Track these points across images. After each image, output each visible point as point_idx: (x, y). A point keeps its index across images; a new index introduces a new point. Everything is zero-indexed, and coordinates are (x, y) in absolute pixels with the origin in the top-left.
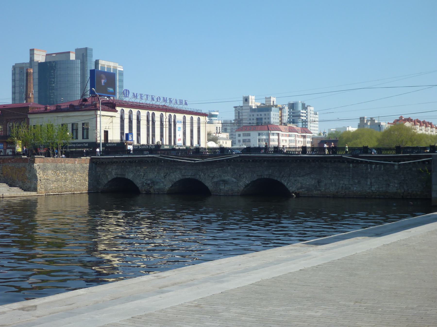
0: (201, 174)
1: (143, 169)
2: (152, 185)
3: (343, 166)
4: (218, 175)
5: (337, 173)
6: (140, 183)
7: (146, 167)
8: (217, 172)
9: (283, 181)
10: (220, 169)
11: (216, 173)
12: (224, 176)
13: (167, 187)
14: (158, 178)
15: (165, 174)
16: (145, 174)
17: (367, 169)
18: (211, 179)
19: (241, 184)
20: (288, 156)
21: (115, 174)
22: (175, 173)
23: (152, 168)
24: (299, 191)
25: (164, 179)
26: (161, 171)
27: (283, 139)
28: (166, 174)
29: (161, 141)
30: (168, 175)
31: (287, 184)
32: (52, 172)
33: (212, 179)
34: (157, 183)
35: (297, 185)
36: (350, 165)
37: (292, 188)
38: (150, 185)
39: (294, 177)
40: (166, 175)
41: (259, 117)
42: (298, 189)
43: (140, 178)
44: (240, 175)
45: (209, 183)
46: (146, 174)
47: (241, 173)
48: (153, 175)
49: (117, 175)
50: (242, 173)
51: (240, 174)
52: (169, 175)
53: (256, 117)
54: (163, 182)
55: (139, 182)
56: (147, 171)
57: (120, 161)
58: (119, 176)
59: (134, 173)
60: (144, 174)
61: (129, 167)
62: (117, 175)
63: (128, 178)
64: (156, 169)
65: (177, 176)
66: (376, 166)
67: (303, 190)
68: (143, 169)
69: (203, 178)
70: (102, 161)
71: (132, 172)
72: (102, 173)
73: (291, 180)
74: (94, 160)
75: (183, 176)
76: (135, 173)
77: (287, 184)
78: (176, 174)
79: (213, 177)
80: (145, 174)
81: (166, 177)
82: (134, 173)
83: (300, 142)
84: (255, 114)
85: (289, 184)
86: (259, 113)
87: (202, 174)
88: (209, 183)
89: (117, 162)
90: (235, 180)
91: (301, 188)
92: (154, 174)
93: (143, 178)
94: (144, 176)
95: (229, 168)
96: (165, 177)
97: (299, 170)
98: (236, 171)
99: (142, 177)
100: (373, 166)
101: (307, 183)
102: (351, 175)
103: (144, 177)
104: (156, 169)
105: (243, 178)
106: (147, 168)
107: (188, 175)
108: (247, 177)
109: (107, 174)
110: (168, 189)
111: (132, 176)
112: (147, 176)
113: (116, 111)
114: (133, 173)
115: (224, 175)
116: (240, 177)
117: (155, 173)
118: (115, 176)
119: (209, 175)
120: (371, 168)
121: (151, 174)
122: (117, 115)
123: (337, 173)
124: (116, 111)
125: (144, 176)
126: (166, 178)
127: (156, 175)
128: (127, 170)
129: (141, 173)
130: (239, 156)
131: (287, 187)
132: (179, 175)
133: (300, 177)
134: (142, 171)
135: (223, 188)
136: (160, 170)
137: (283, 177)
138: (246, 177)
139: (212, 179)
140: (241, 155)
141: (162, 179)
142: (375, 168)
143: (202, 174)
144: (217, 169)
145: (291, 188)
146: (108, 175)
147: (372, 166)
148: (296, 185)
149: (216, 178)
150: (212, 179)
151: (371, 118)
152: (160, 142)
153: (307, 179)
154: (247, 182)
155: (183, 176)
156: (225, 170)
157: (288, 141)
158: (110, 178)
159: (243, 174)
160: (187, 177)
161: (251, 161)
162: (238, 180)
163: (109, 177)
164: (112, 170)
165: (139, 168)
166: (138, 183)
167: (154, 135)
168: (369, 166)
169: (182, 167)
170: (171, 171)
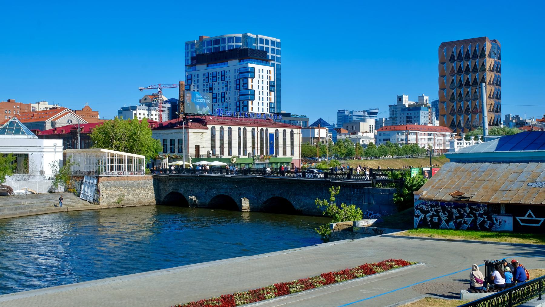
10: (245, 187)
12: (248, 194)
21: (171, 189)
27: (422, 138)
29: (252, 153)
30: (208, 191)
31: (294, 202)
32: (116, 188)
40: (207, 191)
41: (409, 115)
42: (301, 207)
44: (259, 194)
46: (193, 190)
48: (198, 191)
53: (406, 115)
62: (173, 189)
64: (200, 186)
72: (162, 188)
74: (156, 177)
77: (294, 202)
81: (207, 193)
83: (439, 141)
84: (406, 113)
86: (409, 112)
96: (206, 192)
98: (256, 190)
99: (190, 193)
104: (200, 186)
113: (207, 129)
115: (248, 192)
118: (171, 191)
120: (354, 191)
122: (208, 132)
124: (207, 129)
125: (191, 192)
134: (190, 187)
139: (239, 196)
151: (517, 116)
152: (251, 153)
157: (427, 140)
158: (168, 193)
160: (221, 193)
167: (245, 147)
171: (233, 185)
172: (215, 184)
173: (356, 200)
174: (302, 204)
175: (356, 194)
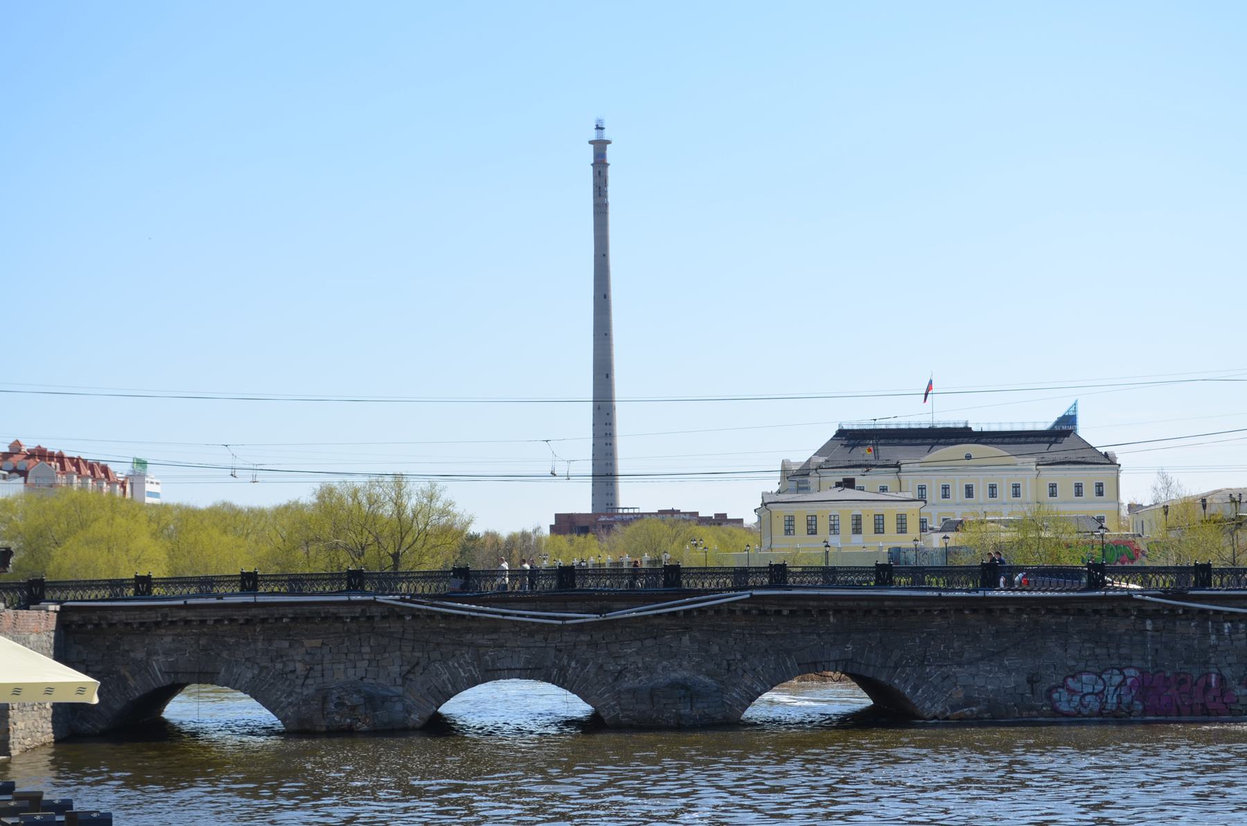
0: (569, 665)
1: (302, 651)
3: (1122, 626)
4: (640, 666)
5: (1098, 651)
6: (290, 704)
7: (317, 643)
8: (638, 654)
9: (897, 681)
10: (648, 642)
11: (631, 659)
12: (664, 668)
15: (403, 668)
16: (311, 669)
17: (1206, 635)
18: (610, 681)
19: (734, 694)
20: (935, 594)
23: (347, 643)
24: (958, 712)
25: (403, 685)
26: (387, 655)
28: (408, 668)
30: (419, 669)
31: (915, 689)
34: (383, 702)
35: (951, 695)
36: (1144, 623)
37: (932, 706)
39: (942, 666)
40: (409, 672)
43: (288, 683)
44: (729, 665)
45: (602, 694)
46: (319, 667)
48: (351, 672)
49: (172, 675)
51: (727, 660)
54: (401, 697)
55: (283, 699)
56: (323, 656)
57: (206, 620)
59: (257, 664)
60: (308, 667)
61: (232, 641)
62: (176, 673)
64: (366, 649)
65: (463, 674)
66: (1235, 629)
67: (974, 709)
68: (302, 651)
70: (67, 623)
71: (247, 659)
73: (928, 678)
74: (76, 618)
75: (487, 671)
76: (263, 664)
77: (915, 689)
78: (456, 665)
79: (620, 672)
80: (311, 669)
81: (411, 676)
82: (257, 664)
85: (920, 691)
87: (573, 664)
88: (602, 694)
89: (187, 622)
91: (968, 702)
92: (355, 667)
93: (303, 685)
94: (307, 677)
95: (686, 639)
96: (404, 677)
97: (956, 644)
98: (715, 649)
99: (300, 682)
100: (1226, 626)
101: (989, 687)
102: (1150, 658)
103: (310, 681)
104: (366, 649)
105: (740, 672)
106: (323, 644)
108: (759, 668)
109: (124, 671)
111: (249, 675)
112: (323, 676)
114: (256, 666)
115: (665, 663)
116: (729, 670)
117: (359, 664)
119: (601, 666)
120: (1219, 632)
121: (342, 666)
123: (1098, 651)
125: (307, 677)
126: (411, 680)
127: (366, 670)
128: (225, 654)
130: (748, 596)
131: (914, 701)
133: (960, 665)
135: (688, 711)
136: (385, 652)
137: (897, 668)
139: (616, 679)
140: (755, 593)
141: (395, 685)
142: (1230, 633)
143: (573, 664)
144: (638, 644)
145: (928, 705)
146: (128, 675)
147: (1223, 626)
148: (946, 692)
149: (628, 675)
150: (616, 679)
153: (990, 672)
156: (671, 647)
159: (744, 658)
161: (785, 612)
162: (722, 682)
163: (132, 683)
164: (149, 654)
165: (286, 644)
166: (282, 702)
168: (1213, 627)
169: (486, 637)
170: (436, 655)
171: (577, 637)
172: (469, 636)
173: (1230, 665)
174: (961, 695)
175: (1232, 641)
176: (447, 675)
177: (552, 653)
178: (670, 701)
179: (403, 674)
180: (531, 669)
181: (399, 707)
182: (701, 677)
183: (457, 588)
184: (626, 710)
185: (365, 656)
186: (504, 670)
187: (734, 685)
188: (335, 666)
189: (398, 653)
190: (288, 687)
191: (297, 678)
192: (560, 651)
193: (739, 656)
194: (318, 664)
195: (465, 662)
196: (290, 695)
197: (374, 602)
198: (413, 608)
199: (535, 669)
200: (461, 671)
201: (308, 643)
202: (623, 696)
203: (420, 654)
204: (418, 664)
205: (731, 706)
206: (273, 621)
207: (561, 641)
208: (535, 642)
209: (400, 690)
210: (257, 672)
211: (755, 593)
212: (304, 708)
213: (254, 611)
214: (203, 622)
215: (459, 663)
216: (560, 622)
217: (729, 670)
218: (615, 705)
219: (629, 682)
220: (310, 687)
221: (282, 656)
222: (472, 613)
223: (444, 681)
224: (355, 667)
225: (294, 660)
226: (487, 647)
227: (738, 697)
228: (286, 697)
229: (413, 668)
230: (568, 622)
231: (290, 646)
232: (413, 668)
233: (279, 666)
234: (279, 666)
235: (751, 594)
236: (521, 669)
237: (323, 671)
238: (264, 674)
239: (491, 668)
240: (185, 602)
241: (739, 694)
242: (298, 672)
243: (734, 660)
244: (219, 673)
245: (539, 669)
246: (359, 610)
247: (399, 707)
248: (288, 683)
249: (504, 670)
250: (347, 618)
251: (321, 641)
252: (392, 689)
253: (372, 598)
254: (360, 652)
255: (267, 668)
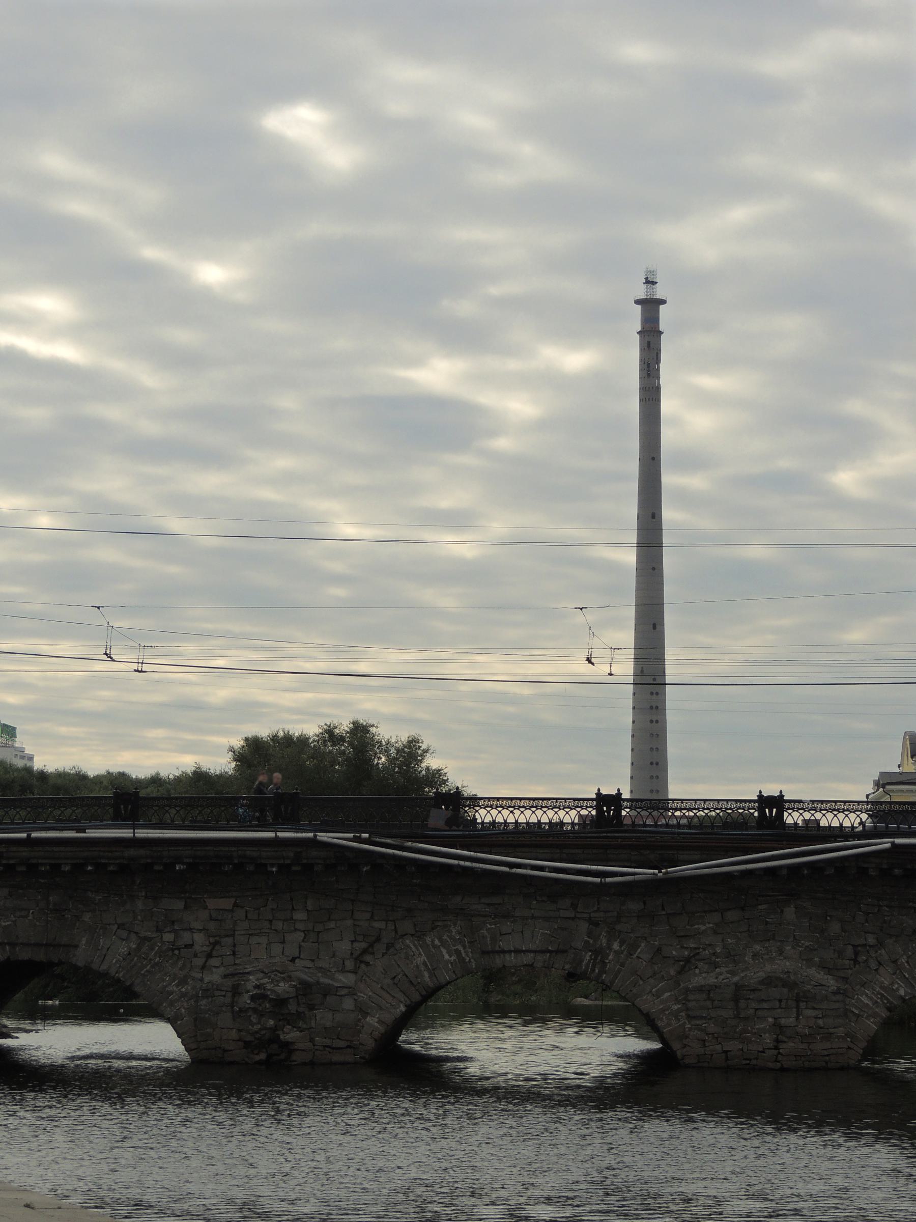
0: (609, 947)
2: (301, 1009)
4: (718, 950)
6: (184, 995)
7: (227, 903)
8: (716, 933)
10: (732, 915)
12: (755, 956)
13: (372, 1021)
14: (310, 964)
15: (356, 945)
16: (214, 944)
18: (672, 973)
19: (864, 999)
22: (428, 940)
26: (332, 925)
28: (364, 945)
33: (679, 973)
34: (325, 996)
38: (292, 1007)
40: (365, 952)
43: (180, 964)
44: (856, 954)
45: (658, 995)
46: (229, 940)
47: (862, 941)
48: (277, 949)
50: (871, 940)
51: (853, 946)
52: (389, 946)
54: (352, 992)
57: (59, 865)
58: (24, 955)
59: (136, 933)
62: (13, 945)
63: (95, 966)
64: (300, 915)
65: (447, 957)
69: (622, 965)
71: (121, 926)
75: (484, 953)
76: (143, 934)
78: (437, 942)
79: (688, 960)
80: (214, 944)
81: (368, 958)
82: (136, 933)
87: (616, 946)
90: (832, 983)
92: (283, 942)
93: (203, 967)
95: (790, 912)
96: (359, 960)
98: (835, 928)
99: (199, 962)
103: (214, 962)
105: (873, 965)
106: (236, 905)
107: (517, 951)
110: (382, 1029)
111: (123, 949)
112: (234, 954)
114: (133, 936)
115: (757, 947)
116: (856, 961)
119: (659, 950)
121: (264, 940)
125: (209, 956)
126: (367, 964)
127: (300, 947)
128: (87, 917)
129: (186, 937)
132: (460, 947)
134: (197, 925)
135: (792, 1021)
136: (329, 920)
138: (895, 962)
140: (898, 841)
141: (343, 971)
143: (616, 946)
149: (701, 964)
154: (902, 992)
155: (484, 953)
156: (767, 923)
159: (881, 944)
162: (845, 979)
165: (180, 905)
166: (171, 993)
169: (483, 900)
176: (424, 958)
177: (584, 926)
178: (765, 1005)
179: (356, 954)
180: (550, 952)
181: (348, 1004)
182: (812, 971)
183: (441, 823)
184: (695, 1017)
185: (300, 926)
186: (510, 952)
187: (863, 985)
188: (254, 940)
189: (349, 922)
190: (181, 969)
191: (196, 956)
192: (597, 924)
193: (871, 940)
194: (228, 936)
195: (450, 937)
196: (183, 982)
197: (314, 842)
198: (373, 852)
199: (557, 952)
200: (444, 951)
201: (212, 903)
202: (691, 997)
203: (382, 925)
204: (378, 939)
205: (858, 1016)
206: (161, 868)
207: (598, 910)
208: (559, 910)
209: (347, 979)
210: (134, 946)
211: (898, 841)
212: (204, 1002)
213: (132, 852)
214: (56, 867)
215: (440, 940)
216: (598, 880)
217: (856, 961)
218: (679, 1011)
219: (699, 978)
220: (214, 970)
221: (173, 922)
222: (462, 863)
223: (417, 966)
224: (283, 942)
225: (190, 930)
226: (485, 916)
227: (870, 1003)
228: (177, 986)
229: (371, 945)
230: (608, 880)
231: (186, 907)
232: (371, 945)
233: (168, 937)
234: (168, 937)
235: (893, 843)
236: (535, 952)
237: (234, 946)
238: (145, 949)
239: (490, 948)
240: (29, 836)
241: (871, 999)
242: (197, 948)
243: (865, 945)
244: (76, 946)
245: (564, 952)
246: (292, 854)
247: (348, 1004)
248: (180, 964)
249: (510, 952)
250: (272, 865)
251: (232, 900)
252: (340, 977)
253: (311, 835)
254: (292, 918)
255: (149, 939)
